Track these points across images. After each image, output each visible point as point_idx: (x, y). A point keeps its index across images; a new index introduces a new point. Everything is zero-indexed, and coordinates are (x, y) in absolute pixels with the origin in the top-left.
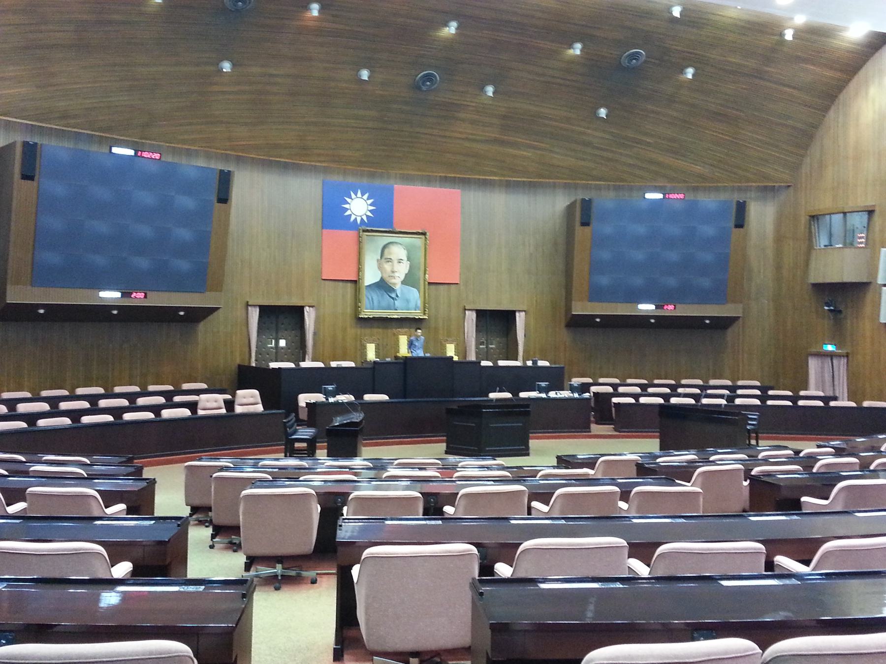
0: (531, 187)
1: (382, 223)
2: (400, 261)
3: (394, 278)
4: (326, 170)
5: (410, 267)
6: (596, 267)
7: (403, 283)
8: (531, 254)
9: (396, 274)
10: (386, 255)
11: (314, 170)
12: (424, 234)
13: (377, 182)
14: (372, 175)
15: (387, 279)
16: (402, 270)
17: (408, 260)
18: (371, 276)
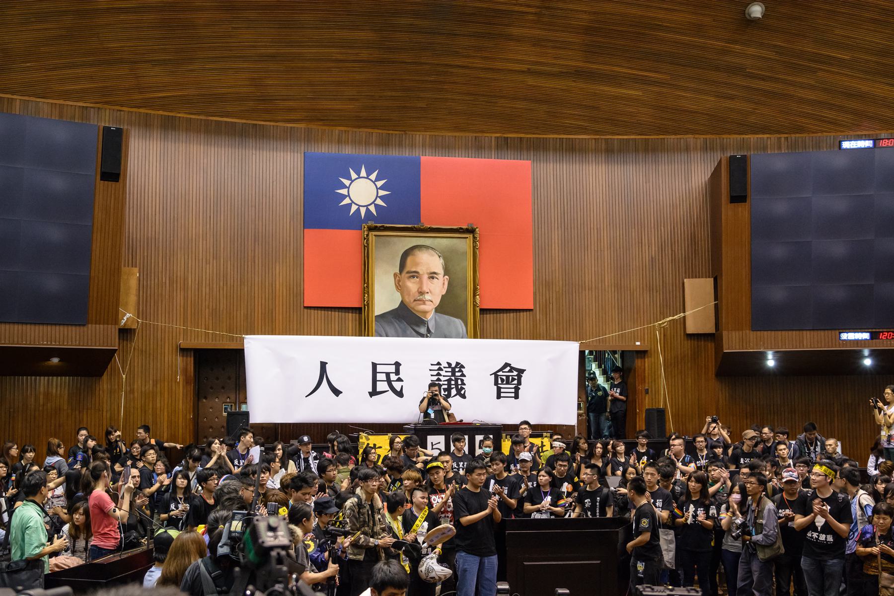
0: (649, 150)
1: (401, 215)
2: (432, 276)
3: (424, 304)
4: (309, 138)
5: (450, 284)
6: (761, 272)
7: (440, 309)
8: (652, 260)
9: (427, 297)
10: (409, 266)
11: (288, 137)
12: (471, 231)
13: (394, 153)
14: (384, 143)
15: (413, 305)
16: (436, 290)
17: (447, 272)
18: (384, 299)
